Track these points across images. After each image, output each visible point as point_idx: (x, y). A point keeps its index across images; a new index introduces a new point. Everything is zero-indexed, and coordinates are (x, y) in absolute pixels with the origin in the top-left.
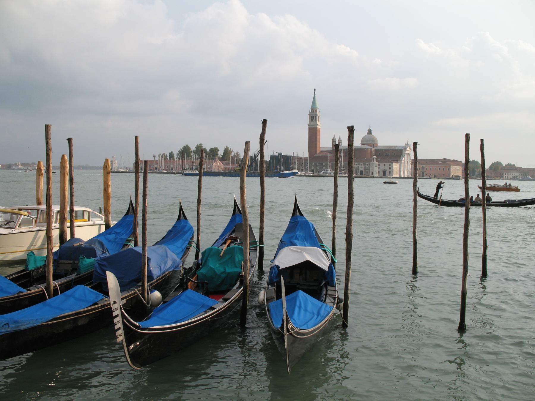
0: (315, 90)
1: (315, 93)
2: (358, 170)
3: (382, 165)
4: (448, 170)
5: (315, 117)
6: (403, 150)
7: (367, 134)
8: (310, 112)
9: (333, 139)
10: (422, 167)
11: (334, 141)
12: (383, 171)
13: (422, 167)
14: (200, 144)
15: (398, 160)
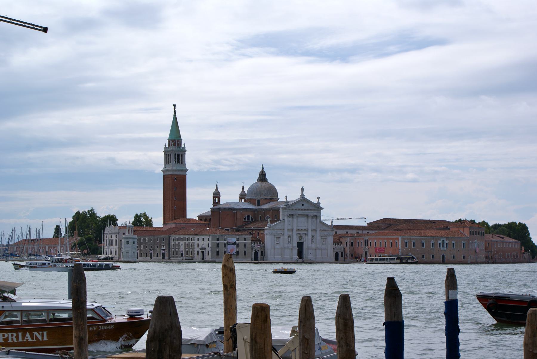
0: (175, 106)
1: (175, 111)
2: (179, 249)
3: (201, 238)
4: (397, 246)
5: (170, 154)
6: (281, 208)
7: (258, 180)
8: (166, 148)
9: (213, 194)
10: (365, 240)
11: (217, 195)
12: (201, 251)
13: (365, 240)
14: (90, 209)
15: (264, 230)
